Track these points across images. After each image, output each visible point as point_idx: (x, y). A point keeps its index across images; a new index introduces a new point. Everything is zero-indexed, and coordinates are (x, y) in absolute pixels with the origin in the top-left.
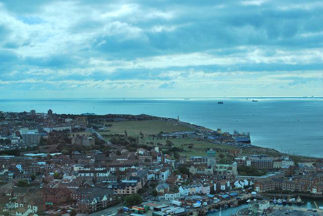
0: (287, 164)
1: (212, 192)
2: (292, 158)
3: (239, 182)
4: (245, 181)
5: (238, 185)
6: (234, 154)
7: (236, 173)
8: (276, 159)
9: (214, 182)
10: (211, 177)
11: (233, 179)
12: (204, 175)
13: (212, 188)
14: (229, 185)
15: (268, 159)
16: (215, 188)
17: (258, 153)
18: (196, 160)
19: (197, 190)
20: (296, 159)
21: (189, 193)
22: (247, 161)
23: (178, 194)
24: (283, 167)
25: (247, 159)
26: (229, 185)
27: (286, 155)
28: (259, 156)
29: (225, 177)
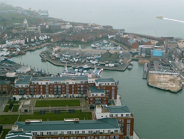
0: (68, 26)
1: (26, 43)
2: (71, 23)
3: (42, 37)
4: (45, 36)
5: (40, 38)
6: (39, 22)
7: (40, 32)
8: (63, 24)
9: (27, 38)
10: (25, 34)
11: (38, 35)
12: (21, 33)
13: (26, 41)
14: (36, 39)
15: (58, 24)
16: (28, 40)
17: (52, 21)
18: (16, 26)
19: (17, 42)
20: (73, 24)
21: (12, 44)
22: (46, 25)
23: (5, 44)
24: (66, 28)
25: (46, 24)
26: (36, 39)
27: (68, 22)
28: (53, 23)
29: (34, 34)
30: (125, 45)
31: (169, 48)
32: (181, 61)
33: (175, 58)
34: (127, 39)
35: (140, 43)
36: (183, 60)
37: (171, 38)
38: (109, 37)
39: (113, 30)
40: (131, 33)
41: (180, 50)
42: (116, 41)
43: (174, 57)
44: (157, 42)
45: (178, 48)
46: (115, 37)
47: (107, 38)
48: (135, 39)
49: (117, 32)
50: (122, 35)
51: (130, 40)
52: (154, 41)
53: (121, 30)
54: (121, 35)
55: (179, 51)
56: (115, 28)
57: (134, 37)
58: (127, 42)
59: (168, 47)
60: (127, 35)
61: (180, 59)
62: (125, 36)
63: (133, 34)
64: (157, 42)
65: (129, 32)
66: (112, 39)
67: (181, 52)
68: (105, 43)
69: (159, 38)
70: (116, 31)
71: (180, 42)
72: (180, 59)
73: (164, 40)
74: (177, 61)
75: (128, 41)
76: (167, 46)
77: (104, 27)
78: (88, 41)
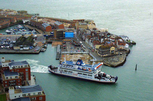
30: (40, 29)
31: (80, 30)
32: (90, 40)
33: (85, 39)
34: (41, 23)
35: (53, 26)
36: (92, 40)
37: (82, 21)
38: (24, 22)
39: (27, 14)
40: (45, 18)
41: (89, 31)
42: (30, 25)
43: (84, 37)
44: (69, 25)
45: (87, 29)
46: (30, 21)
47: (21, 23)
48: (49, 23)
49: (31, 17)
50: (37, 19)
51: (44, 24)
52: (66, 24)
53: (36, 14)
54: (36, 20)
55: (89, 32)
56: (29, 12)
57: (48, 21)
58: (42, 25)
59: (79, 29)
60: (41, 20)
61: (89, 40)
62: (39, 20)
63: (47, 18)
64: (69, 25)
65: (44, 16)
66: (27, 23)
67: (90, 32)
68: (20, 28)
69: (71, 21)
70: (31, 16)
71: (90, 24)
72: (89, 40)
73: (76, 22)
74: (87, 41)
75: (43, 25)
76: (78, 28)
77: (18, 12)
78: (2, 26)
